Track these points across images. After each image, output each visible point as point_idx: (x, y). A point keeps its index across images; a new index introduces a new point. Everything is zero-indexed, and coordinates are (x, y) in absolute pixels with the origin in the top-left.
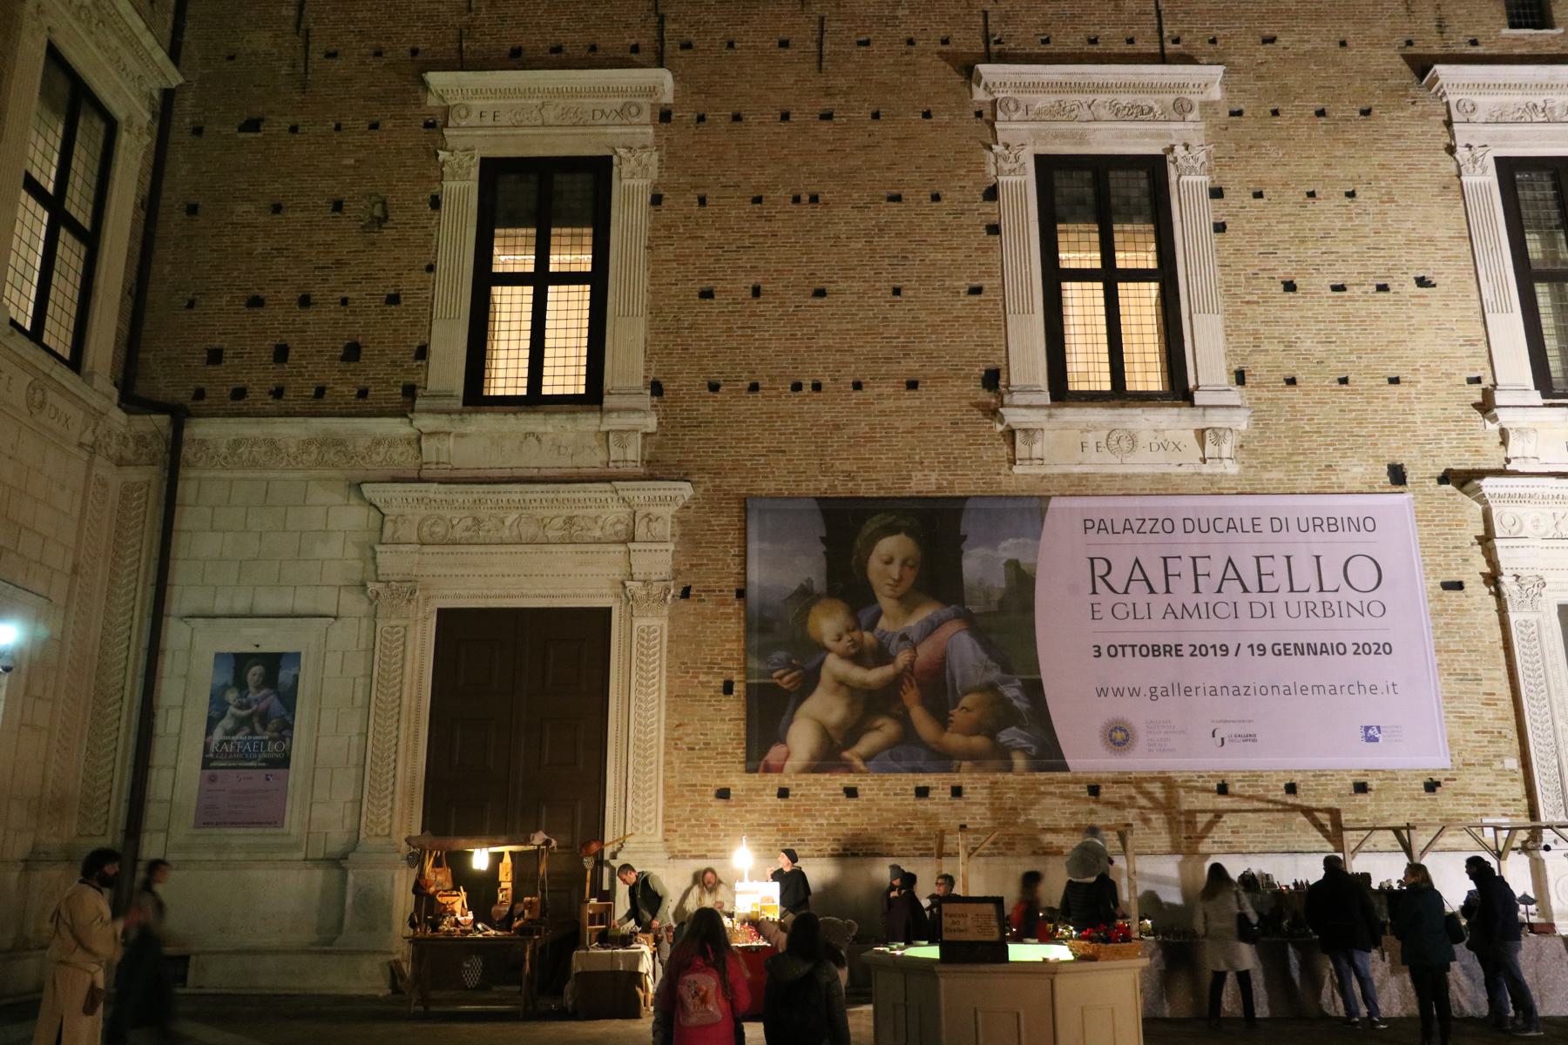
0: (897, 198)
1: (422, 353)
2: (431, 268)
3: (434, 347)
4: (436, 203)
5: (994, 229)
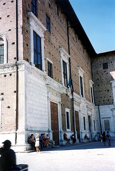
1: (113, 100)
2: (113, 94)
3: (114, 99)
4: (112, 90)
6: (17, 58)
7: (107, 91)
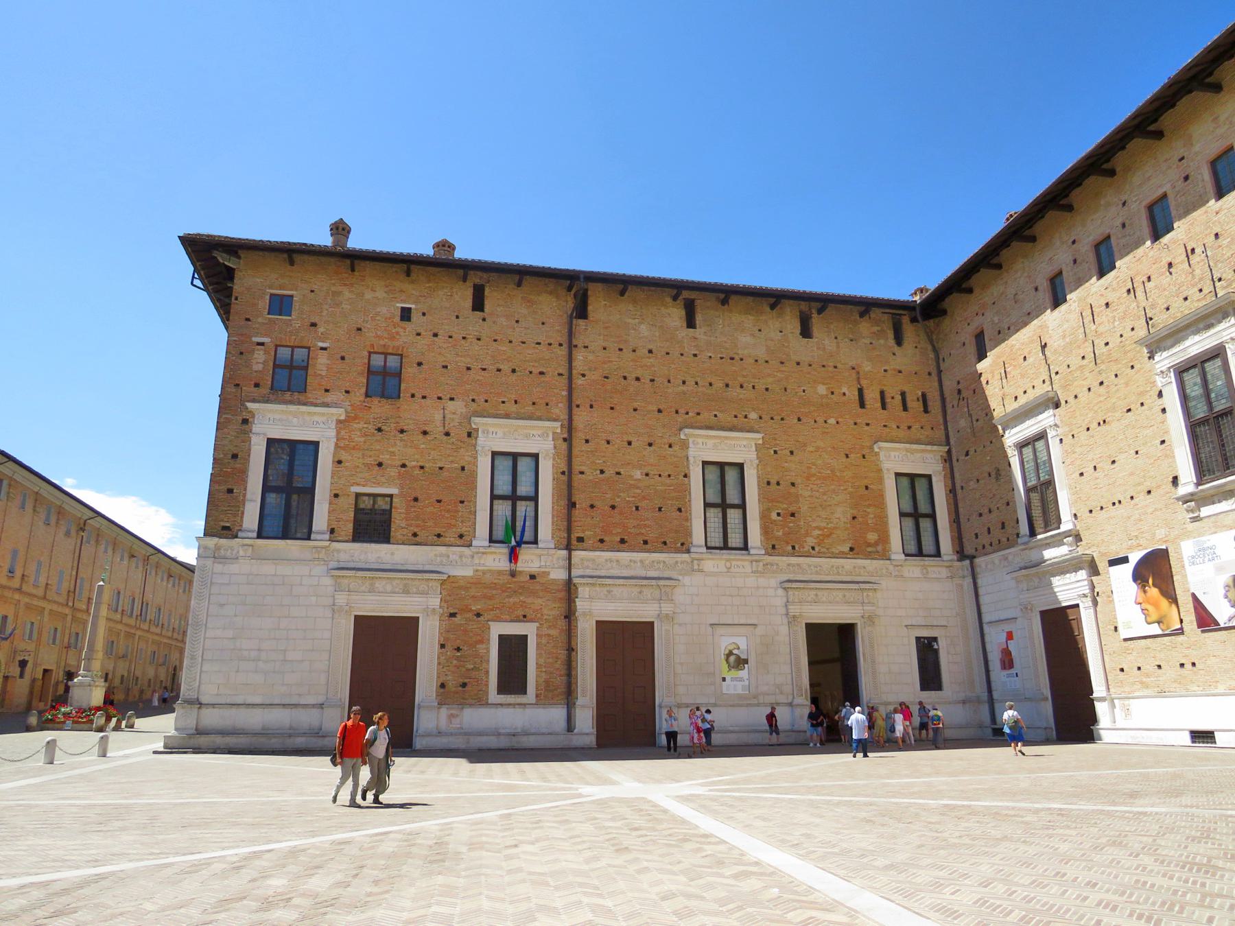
0: (1129, 410)
5: (1164, 410)
7: (993, 474)
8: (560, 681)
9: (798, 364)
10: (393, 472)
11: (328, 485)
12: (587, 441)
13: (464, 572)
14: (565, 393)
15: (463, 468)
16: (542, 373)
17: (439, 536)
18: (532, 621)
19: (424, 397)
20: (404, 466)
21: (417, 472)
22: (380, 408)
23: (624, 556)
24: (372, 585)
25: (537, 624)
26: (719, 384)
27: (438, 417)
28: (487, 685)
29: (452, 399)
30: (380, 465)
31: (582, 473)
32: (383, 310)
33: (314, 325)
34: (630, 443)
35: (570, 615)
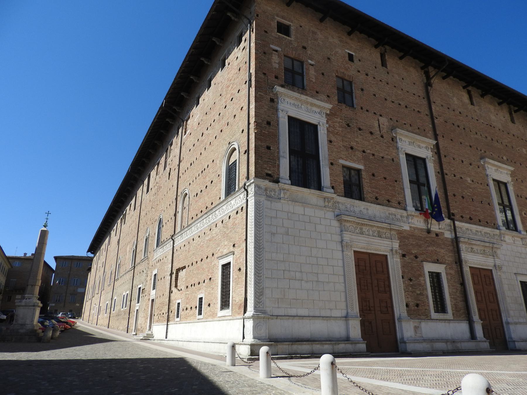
6: (248, 178)
8: (461, 304)
9: (514, 135)
10: (359, 154)
11: (327, 156)
12: (445, 156)
13: (406, 227)
14: (431, 126)
15: (393, 160)
16: (419, 112)
17: (389, 201)
18: (441, 263)
19: (367, 111)
20: (364, 152)
21: (371, 157)
22: (346, 111)
23: (474, 227)
24: (361, 229)
25: (445, 266)
26: (489, 138)
27: (377, 125)
28: (429, 306)
29: (381, 116)
30: (352, 148)
31: (446, 174)
32: (340, 51)
33: (304, 48)
34: (462, 162)
35: (459, 261)
